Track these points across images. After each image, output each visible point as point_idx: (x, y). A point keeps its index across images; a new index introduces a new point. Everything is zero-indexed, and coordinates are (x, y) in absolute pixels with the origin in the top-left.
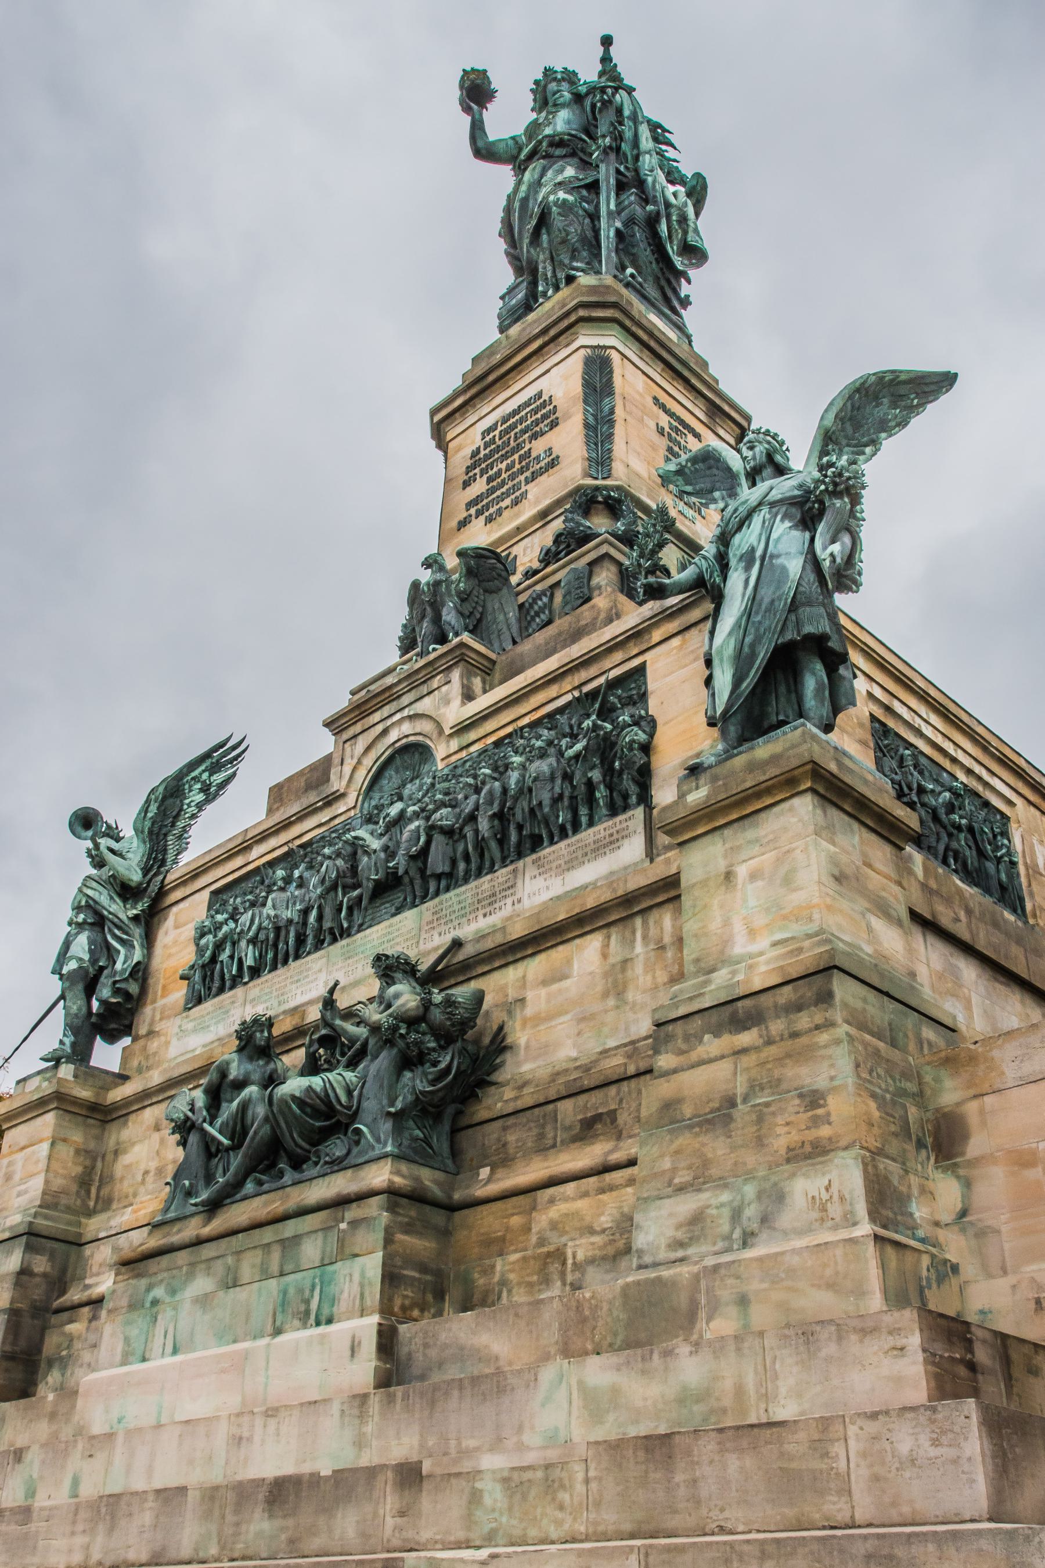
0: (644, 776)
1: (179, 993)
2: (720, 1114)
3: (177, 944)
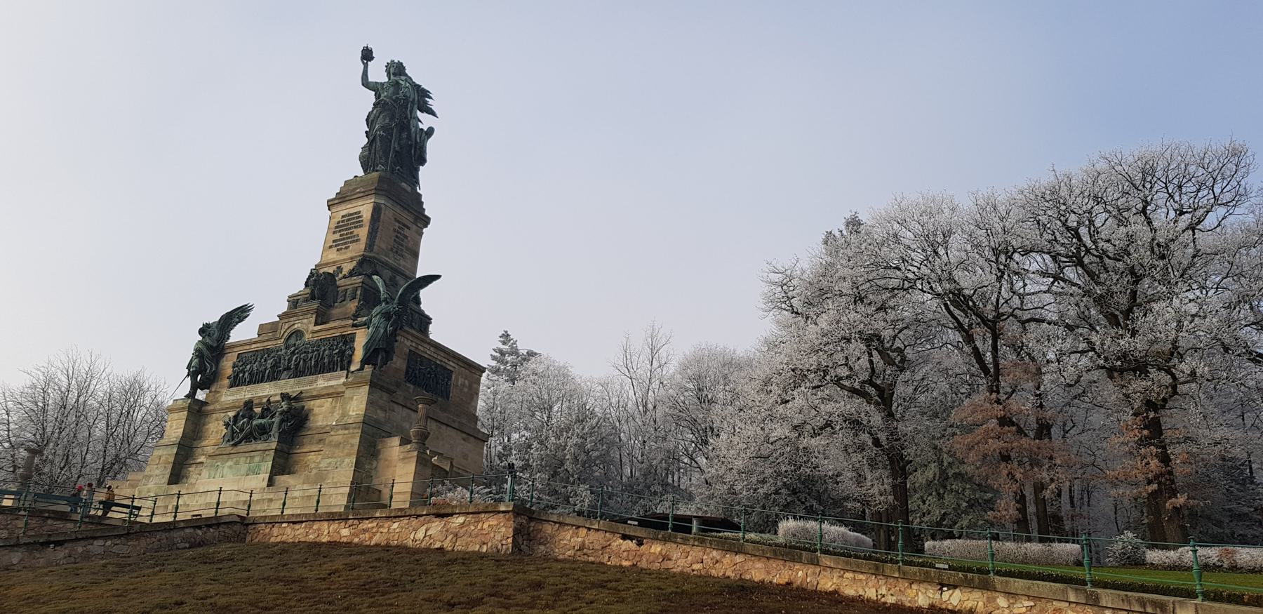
0: (350, 362)
1: (227, 382)
2: (338, 445)
3: (228, 365)
